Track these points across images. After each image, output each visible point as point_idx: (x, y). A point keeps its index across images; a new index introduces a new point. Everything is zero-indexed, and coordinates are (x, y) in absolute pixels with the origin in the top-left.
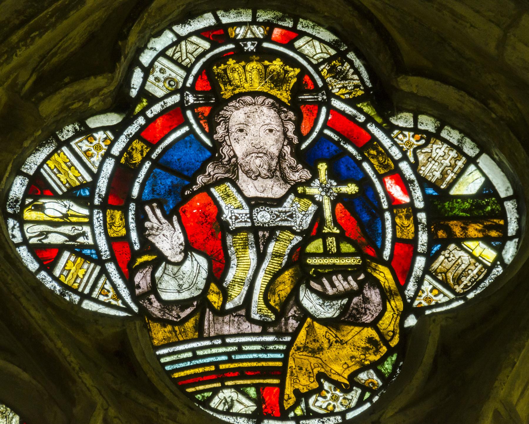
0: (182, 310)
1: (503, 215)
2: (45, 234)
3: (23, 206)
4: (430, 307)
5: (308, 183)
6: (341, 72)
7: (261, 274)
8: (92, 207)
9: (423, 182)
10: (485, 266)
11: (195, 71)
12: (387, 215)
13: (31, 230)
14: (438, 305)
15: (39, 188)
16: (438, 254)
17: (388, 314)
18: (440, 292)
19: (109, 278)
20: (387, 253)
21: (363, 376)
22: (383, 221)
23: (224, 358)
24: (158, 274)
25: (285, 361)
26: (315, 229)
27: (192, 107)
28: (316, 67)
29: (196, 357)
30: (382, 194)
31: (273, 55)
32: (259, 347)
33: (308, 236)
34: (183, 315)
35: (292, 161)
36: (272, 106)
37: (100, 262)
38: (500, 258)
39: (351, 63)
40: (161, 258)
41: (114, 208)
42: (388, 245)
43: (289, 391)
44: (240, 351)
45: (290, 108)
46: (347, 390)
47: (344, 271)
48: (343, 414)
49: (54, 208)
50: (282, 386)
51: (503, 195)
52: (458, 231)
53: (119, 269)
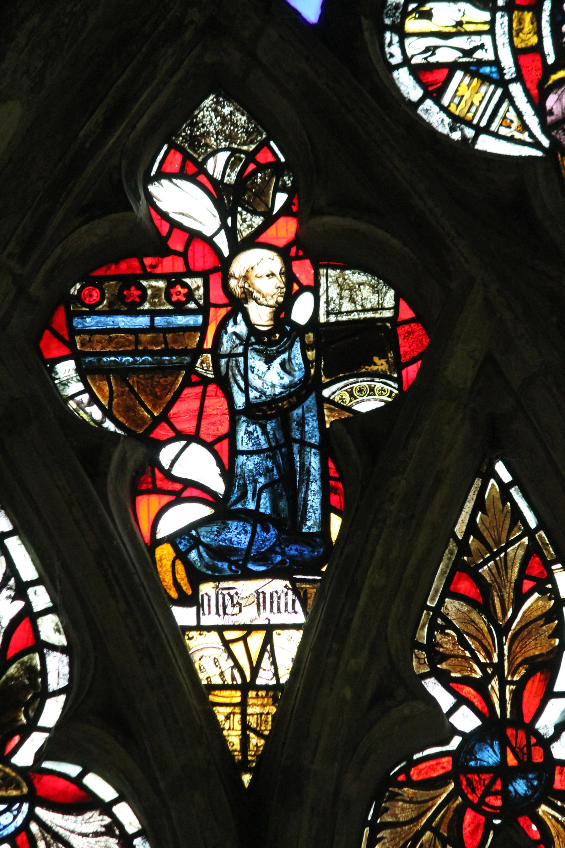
2: (432, 50)
3: (405, 14)
8: (494, 9)
13: (414, 46)
19: (512, 103)
37: (502, 83)
41: (522, 8)
53: (527, 91)
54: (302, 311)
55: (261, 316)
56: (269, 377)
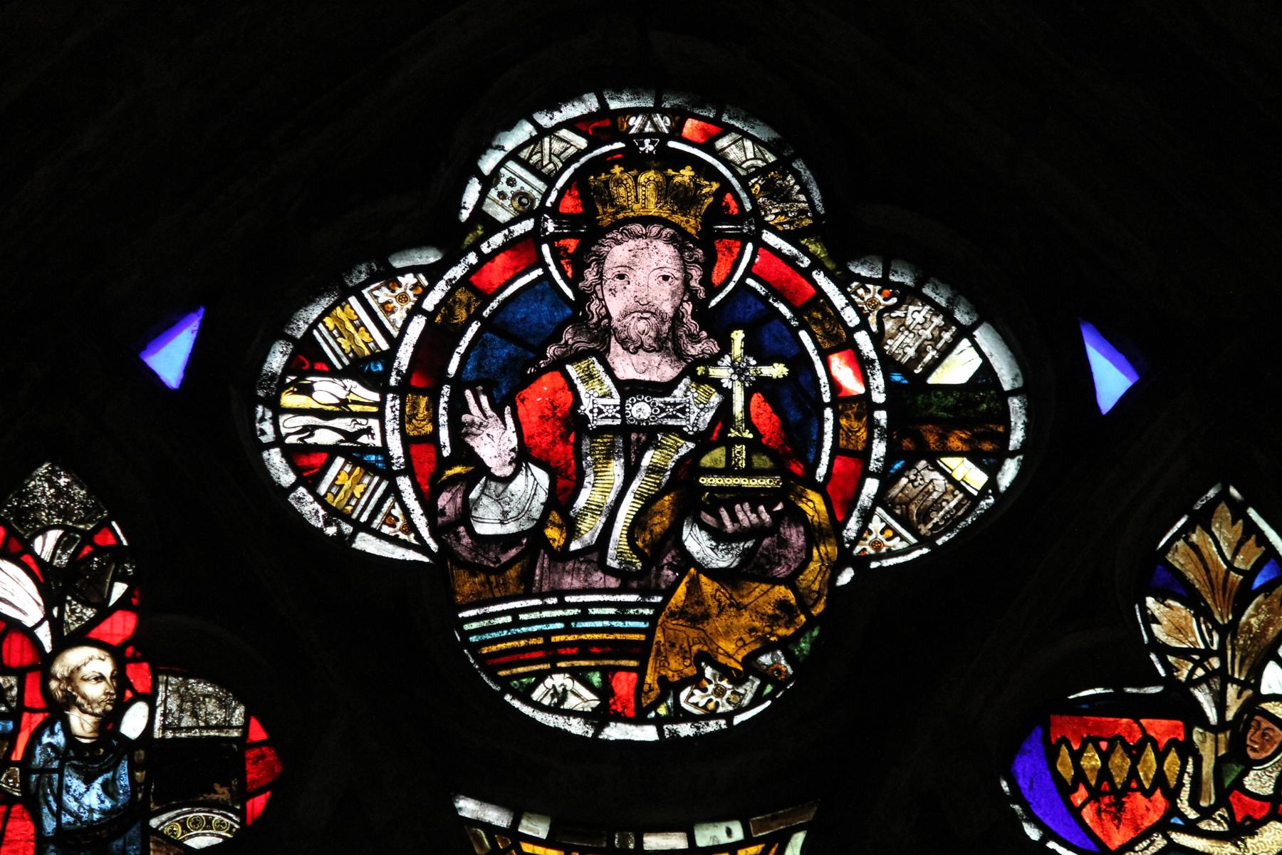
0: (505, 550)
1: (1004, 417)
2: (310, 430)
3: (282, 387)
4: (879, 557)
5: (713, 360)
6: (782, 189)
7: (629, 498)
9: (889, 363)
10: (967, 495)
11: (560, 183)
12: (828, 413)
13: (290, 424)
14: (891, 553)
15: (308, 360)
16: (900, 474)
17: (814, 566)
18: (896, 534)
20: (822, 470)
21: (766, 659)
22: (822, 420)
23: (559, 626)
24: (474, 495)
25: (649, 632)
26: (718, 431)
27: (551, 239)
28: (744, 181)
29: (517, 623)
30: (824, 380)
31: (682, 160)
32: (612, 611)
33: (704, 441)
34: (504, 559)
35: (693, 326)
36: (671, 240)
37: (388, 474)
38: (992, 484)
39: (797, 175)
40: (480, 470)
41: (418, 392)
42: (825, 459)
43: (650, 679)
44: (585, 616)
45: (698, 244)
46: (738, 680)
47: (754, 498)
48: (728, 716)
49: (327, 391)
50: (641, 671)
51: (1007, 387)
52: (932, 440)
54: (134, 723)
55: (82, 724)
56: (89, 799)
